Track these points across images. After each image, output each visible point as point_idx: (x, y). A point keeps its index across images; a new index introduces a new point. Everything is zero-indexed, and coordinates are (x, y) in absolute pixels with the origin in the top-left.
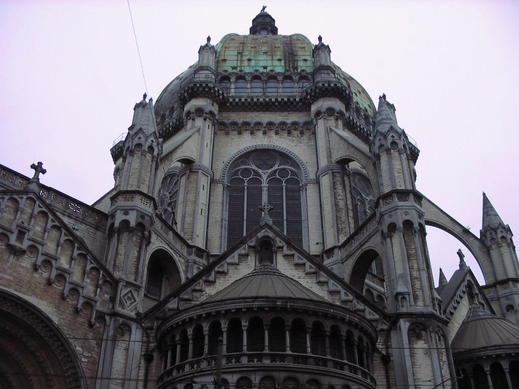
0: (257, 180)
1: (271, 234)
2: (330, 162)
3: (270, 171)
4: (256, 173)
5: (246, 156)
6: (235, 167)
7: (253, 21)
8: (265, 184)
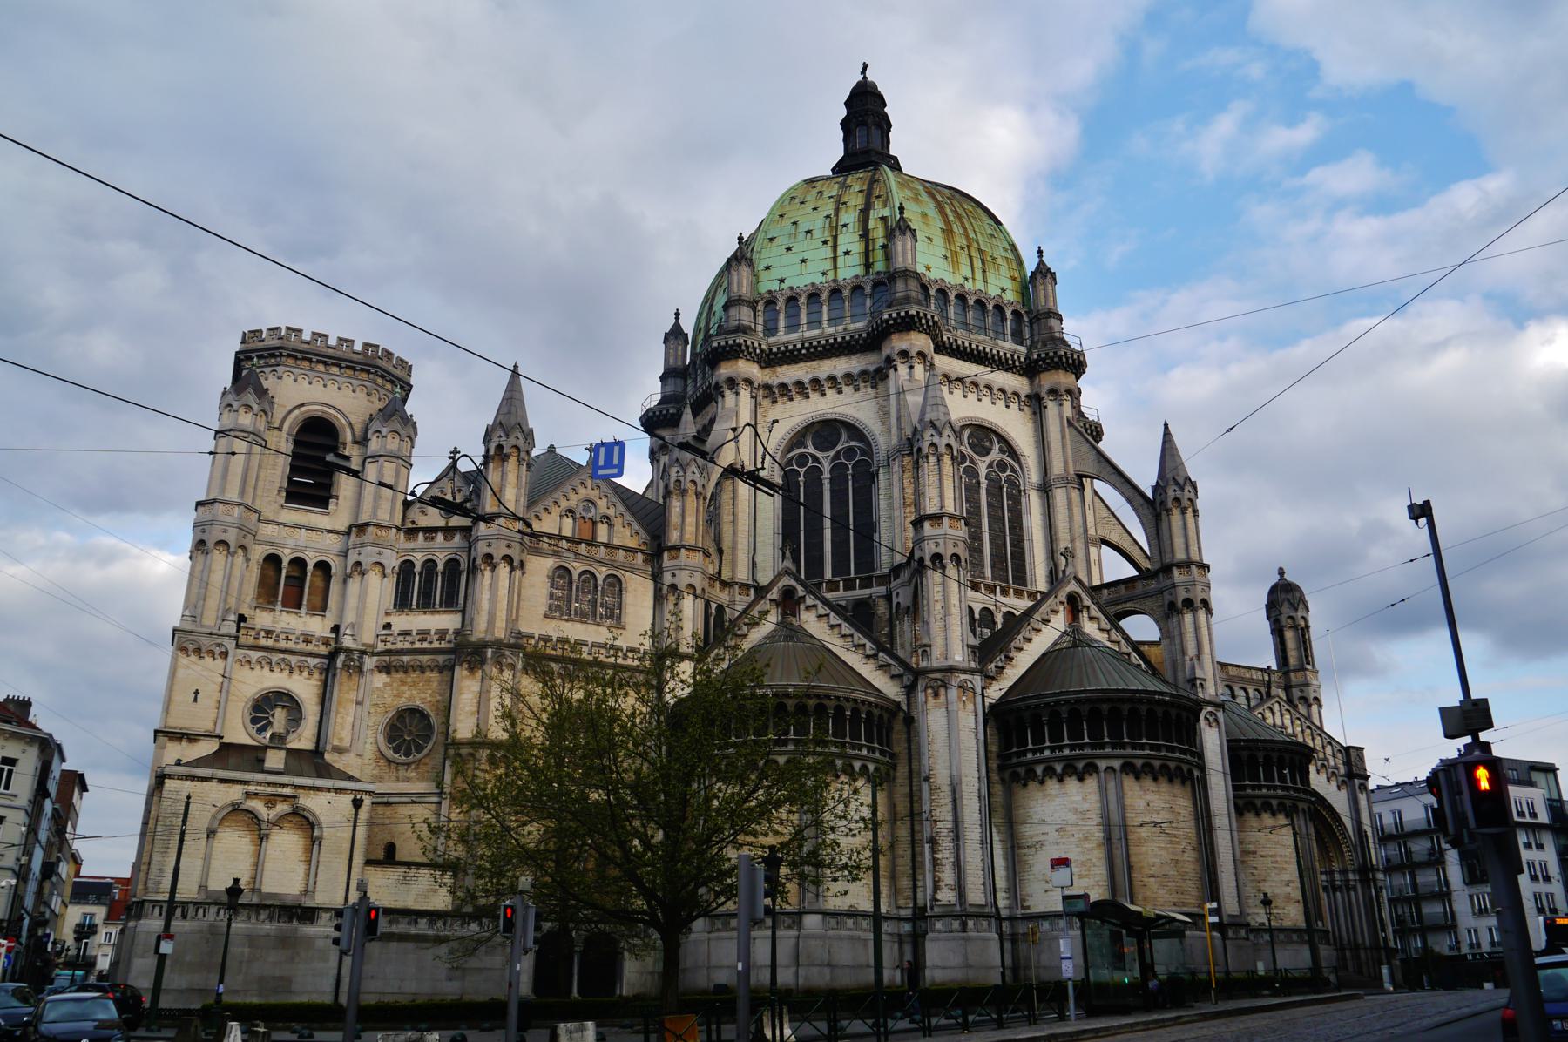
0: (814, 474)
1: (793, 583)
2: (900, 439)
3: (832, 453)
4: (815, 459)
5: (798, 439)
6: (789, 452)
7: (846, 104)
8: (826, 475)
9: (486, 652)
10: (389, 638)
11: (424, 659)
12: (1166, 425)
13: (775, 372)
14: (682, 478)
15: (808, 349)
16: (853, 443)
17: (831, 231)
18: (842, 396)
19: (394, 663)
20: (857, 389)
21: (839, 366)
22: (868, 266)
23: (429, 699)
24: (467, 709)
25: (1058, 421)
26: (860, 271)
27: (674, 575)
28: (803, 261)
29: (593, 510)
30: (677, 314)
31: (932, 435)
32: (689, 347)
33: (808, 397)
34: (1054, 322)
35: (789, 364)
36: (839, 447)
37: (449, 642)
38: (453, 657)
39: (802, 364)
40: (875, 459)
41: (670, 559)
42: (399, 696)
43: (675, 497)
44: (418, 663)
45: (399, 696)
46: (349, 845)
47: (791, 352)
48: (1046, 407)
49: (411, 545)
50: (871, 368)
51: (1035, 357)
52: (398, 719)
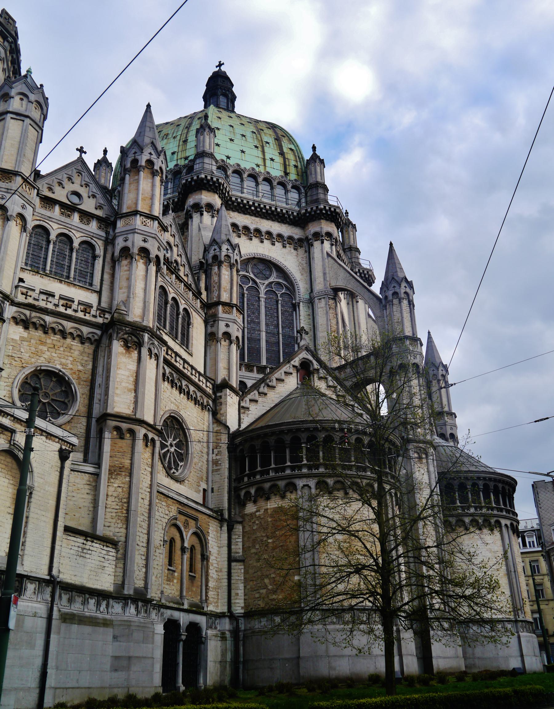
1: (311, 358)
3: (267, 282)
8: (262, 295)
9: (143, 336)
10: (30, 293)
11: (68, 325)
12: (429, 332)
13: (229, 214)
14: (231, 255)
15: (256, 208)
16: (280, 281)
17: (259, 142)
18: (273, 247)
19: (34, 320)
20: (284, 247)
21: (276, 228)
22: (286, 174)
23: (70, 366)
24: (124, 384)
25: (364, 312)
26: (282, 174)
27: (227, 326)
28: (243, 152)
29: (169, 252)
30: (105, 152)
31: (394, 287)
32: (112, 177)
33: (251, 239)
34: (357, 253)
35: (239, 212)
36: (271, 280)
37: (95, 316)
38: (99, 332)
39: (248, 216)
40: (297, 296)
41: (224, 312)
42: (37, 354)
43: (224, 267)
44: (61, 328)
45: (37, 354)
46: (53, 503)
47: (244, 205)
48: (357, 302)
49: (48, 213)
50: (296, 237)
51: (357, 270)
52: (31, 377)
